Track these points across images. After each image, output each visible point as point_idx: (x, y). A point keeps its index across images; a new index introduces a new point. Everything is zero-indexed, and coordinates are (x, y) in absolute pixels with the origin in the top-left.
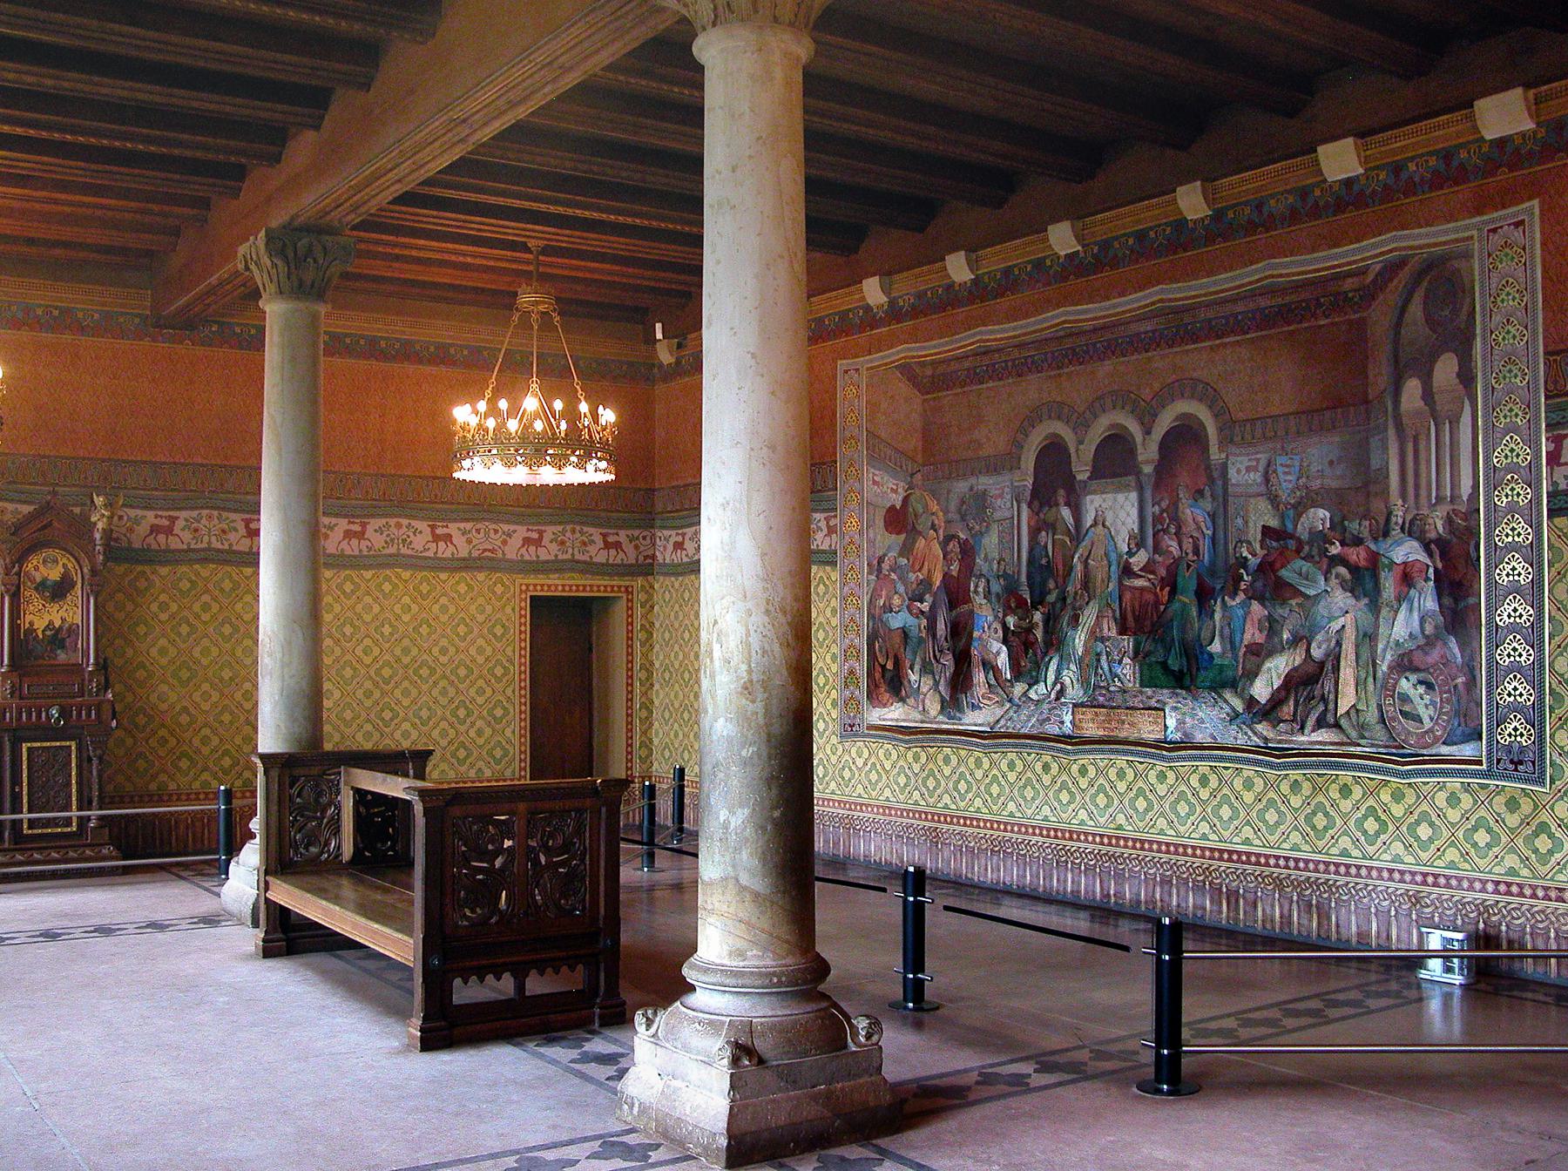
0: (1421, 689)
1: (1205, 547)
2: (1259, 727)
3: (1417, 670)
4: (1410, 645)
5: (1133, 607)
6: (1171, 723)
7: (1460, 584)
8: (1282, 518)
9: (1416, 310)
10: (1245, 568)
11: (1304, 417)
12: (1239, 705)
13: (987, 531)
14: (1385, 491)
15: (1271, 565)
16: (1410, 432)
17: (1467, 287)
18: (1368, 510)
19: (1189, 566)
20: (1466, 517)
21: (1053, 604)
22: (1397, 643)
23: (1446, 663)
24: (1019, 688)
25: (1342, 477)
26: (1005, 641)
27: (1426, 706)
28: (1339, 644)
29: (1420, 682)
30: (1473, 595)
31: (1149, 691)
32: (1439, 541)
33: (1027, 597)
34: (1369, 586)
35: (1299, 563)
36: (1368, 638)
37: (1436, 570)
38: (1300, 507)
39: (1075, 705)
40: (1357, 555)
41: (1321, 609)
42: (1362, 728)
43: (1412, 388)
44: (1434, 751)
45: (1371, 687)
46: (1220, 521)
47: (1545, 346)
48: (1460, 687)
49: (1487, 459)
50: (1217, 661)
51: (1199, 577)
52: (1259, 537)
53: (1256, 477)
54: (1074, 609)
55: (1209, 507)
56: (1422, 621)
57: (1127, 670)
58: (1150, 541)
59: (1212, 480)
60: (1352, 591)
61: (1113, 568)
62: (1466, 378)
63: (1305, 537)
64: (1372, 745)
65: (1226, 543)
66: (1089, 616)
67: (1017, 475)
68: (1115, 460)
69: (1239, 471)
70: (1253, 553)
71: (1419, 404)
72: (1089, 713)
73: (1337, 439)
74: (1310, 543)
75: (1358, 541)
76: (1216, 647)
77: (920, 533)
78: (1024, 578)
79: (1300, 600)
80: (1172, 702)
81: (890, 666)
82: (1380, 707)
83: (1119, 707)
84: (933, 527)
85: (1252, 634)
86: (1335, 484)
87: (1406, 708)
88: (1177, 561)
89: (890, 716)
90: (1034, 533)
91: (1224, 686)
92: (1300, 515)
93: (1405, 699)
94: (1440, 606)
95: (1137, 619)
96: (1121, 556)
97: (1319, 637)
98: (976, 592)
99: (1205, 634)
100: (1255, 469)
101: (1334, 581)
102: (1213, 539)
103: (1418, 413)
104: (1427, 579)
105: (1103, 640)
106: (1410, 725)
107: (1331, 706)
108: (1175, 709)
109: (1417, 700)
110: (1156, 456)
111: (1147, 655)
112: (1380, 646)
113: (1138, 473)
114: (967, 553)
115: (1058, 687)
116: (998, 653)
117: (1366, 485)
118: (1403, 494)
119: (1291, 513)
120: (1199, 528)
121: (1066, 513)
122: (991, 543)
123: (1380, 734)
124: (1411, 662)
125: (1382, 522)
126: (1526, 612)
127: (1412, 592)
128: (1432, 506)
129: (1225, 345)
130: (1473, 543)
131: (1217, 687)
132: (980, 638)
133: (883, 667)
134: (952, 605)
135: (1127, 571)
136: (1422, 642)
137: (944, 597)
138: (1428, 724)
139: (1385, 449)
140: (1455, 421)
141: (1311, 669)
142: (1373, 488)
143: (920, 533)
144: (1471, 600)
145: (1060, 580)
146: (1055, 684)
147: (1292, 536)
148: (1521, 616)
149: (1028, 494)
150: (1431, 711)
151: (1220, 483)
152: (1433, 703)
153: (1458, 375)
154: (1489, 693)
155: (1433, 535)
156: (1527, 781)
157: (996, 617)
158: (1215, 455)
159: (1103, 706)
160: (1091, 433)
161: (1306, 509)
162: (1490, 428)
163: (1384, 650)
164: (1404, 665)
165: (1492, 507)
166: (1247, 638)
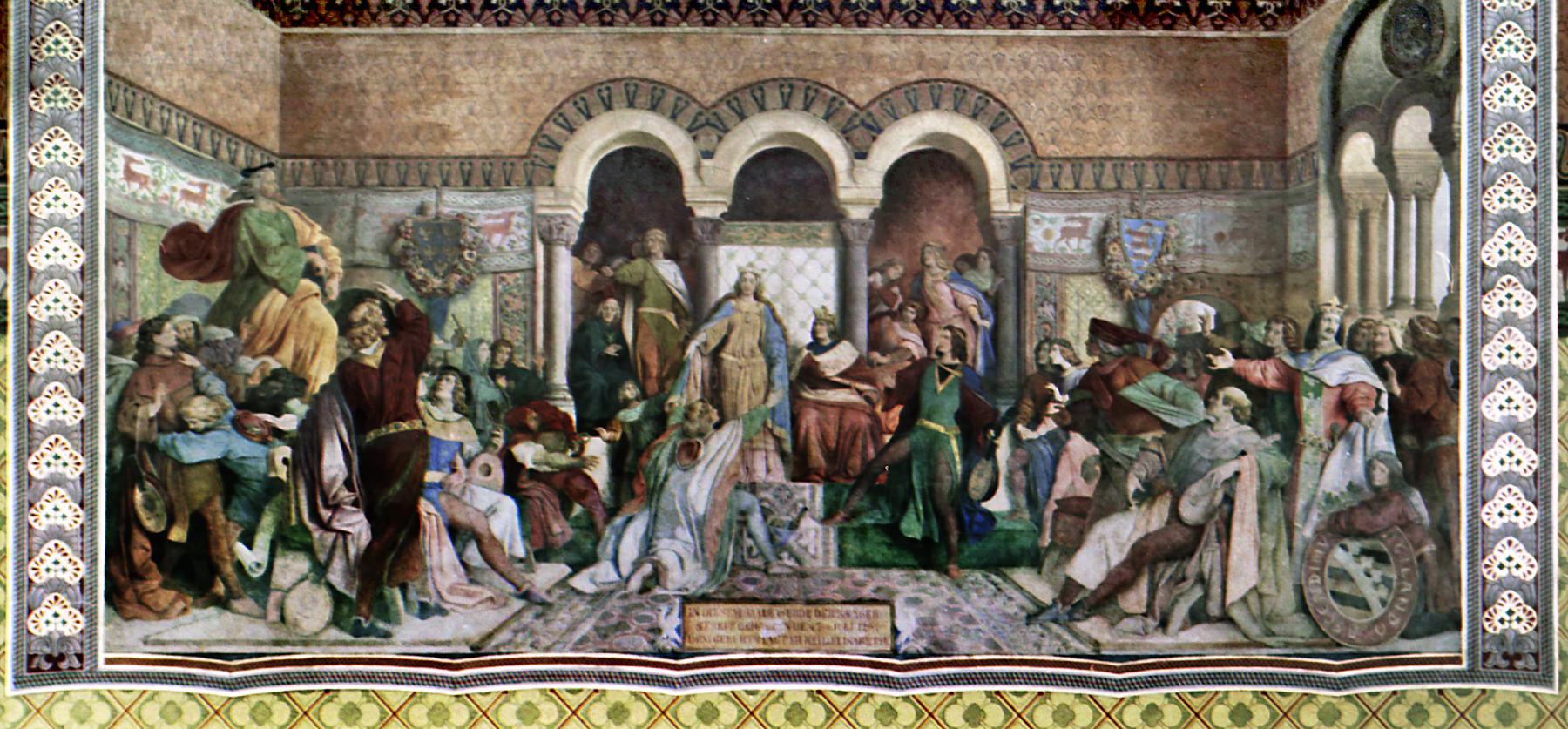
0: (1367, 562)
1: (976, 348)
2: (1084, 626)
3: (1361, 535)
4: (1348, 501)
5: (824, 440)
6: (907, 622)
7: (1427, 418)
8: (1131, 309)
9: (1369, 38)
10: (1059, 382)
11: (1172, 166)
12: (1044, 592)
13: (465, 286)
14: (1313, 285)
15: (1108, 379)
16: (1355, 208)
17: (1450, 21)
18: (1283, 309)
19: (944, 375)
20: (1439, 327)
21: (635, 426)
22: (1329, 499)
23: (1407, 524)
24: (547, 575)
25: (1240, 259)
26: (510, 488)
27: (1376, 585)
28: (1229, 500)
29: (1365, 552)
30: (1447, 433)
31: (860, 574)
32: (1397, 358)
33: (569, 408)
34: (1282, 417)
35: (1156, 380)
36: (1281, 489)
37: (1391, 396)
38: (1162, 298)
39: (686, 600)
40: (1264, 373)
41: (1199, 447)
42: (1267, 620)
43: (1359, 151)
44: (1387, 648)
45: (1284, 561)
46: (1009, 308)
47: (1560, 117)
48: (1430, 559)
49: (1474, 254)
50: (1001, 524)
51: (964, 390)
52: (1085, 336)
53: (1083, 246)
54: (685, 433)
55: (987, 284)
56: (1369, 467)
57: (815, 539)
58: (862, 330)
59: (993, 246)
60: (1253, 423)
61: (781, 369)
62: (1444, 141)
63: (1171, 340)
64: (1287, 645)
65: (1020, 343)
66: (722, 446)
67: (544, 197)
68: (785, 191)
69: (1047, 234)
70: (1076, 361)
71: (1372, 169)
72: (720, 614)
73: (1231, 204)
74: (1181, 350)
75: (1265, 353)
76: (999, 504)
77: (273, 283)
78: (560, 377)
79: (1159, 434)
80: (908, 591)
81: (178, 534)
82: (1299, 590)
83: (790, 601)
84: (311, 272)
85: (1070, 482)
86: (1225, 268)
87: (1345, 589)
88: (920, 366)
90: (589, 302)
91: (1014, 562)
92: (1163, 309)
93: (1342, 575)
94: (1398, 445)
95: (832, 455)
96: (797, 351)
97: (1194, 489)
98: (433, 398)
99: (978, 483)
100: (1081, 233)
101: (1220, 409)
102: (995, 334)
103: (1368, 182)
104: (1378, 410)
105: (753, 488)
106: (1351, 613)
107: (1216, 590)
108: (915, 602)
109: (1359, 576)
110: (878, 195)
111: (854, 514)
112: (1301, 502)
113: (836, 216)
114: (409, 330)
115: (647, 569)
116: (493, 510)
117: (1279, 275)
118: (1341, 290)
119: (1146, 304)
120: (964, 313)
121: (670, 272)
122: (474, 311)
123: (1299, 628)
124: (1349, 523)
125: (1305, 323)
126: (1528, 458)
127: (1355, 428)
128: (1388, 311)
129: (1029, 39)
130: (1448, 363)
131: (1001, 561)
132: (440, 485)
134: (360, 424)
135: (810, 376)
136: (1368, 494)
138: (1378, 611)
139: (1312, 221)
140: (1425, 198)
141: (1179, 536)
142: (1290, 279)
144: (1445, 441)
145: (652, 386)
146: (637, 565)
147: (1146, 339)
148: (1519, 462)
149: (573, 232)
150: (1383, 592)
151: (1011, 248)
152: (1386, 581)
153: (1432, 137)
154: (1472, 564)
155: (1387, 349)
156: (1528, 681)
157: (486, 445)
158: (1001, 201)
159: (754, 601)
160: (731, 141)
161: (1172, 300)
162: (1480, 213)
163: (1308, 509)
164: (1340, 526)
165: (1478, 317)
166: (1062, 488)
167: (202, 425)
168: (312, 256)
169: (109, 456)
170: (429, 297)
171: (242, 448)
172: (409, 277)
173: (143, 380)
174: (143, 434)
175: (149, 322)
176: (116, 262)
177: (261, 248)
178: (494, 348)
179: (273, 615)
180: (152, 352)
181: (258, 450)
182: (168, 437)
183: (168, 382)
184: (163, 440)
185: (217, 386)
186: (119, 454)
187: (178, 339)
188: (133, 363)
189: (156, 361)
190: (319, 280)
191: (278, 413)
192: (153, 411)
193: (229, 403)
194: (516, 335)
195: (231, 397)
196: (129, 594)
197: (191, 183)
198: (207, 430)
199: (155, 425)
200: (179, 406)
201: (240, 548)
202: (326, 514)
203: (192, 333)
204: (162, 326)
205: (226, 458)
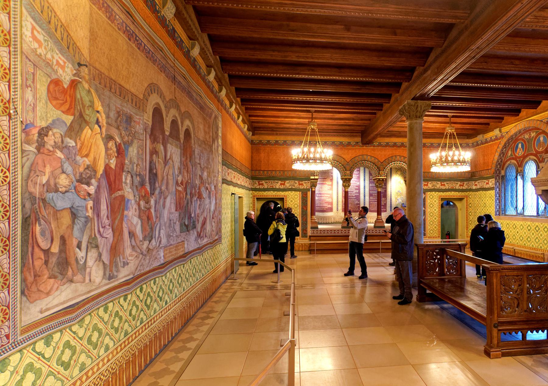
77: (87, 123)
81: (55, 249)
84: (98, 122)
89: (55, 302)
98: (126, 183)
133: (47, 252)
137: (104, 183)
143: (87, 123)
157: (136, 201)
167: (64, 189)
168: (98, 115)
169: (23, 206)
170: (125, 143)
171: (78, 202)
172: (121, 134)
173: (40, 162)
174: (40, 193)
175: (43, 129)
176: (27, 87)
177: (84, 106)
178: (137, 166)
179: (87, 280)
180: (44, 146)
181: (83, 203)
182: (51, 194)
183: (51, 165)
184: (49, 196)
185: (68, 168)
186: (28, 205)
187: (55, 142)
188: (35, 151)
189: (46, 151)
190: (100, 126)
191: (88, 184)
192: (44, 180)
193: (74, 179)
194: (140, 163)
195: (75, 175)
196: (34, 288)
197: (60, 58)
198: (66, 192)
199: (45, 187)
200: (55, 179)
201: (77, 249)
202: (101, 230)
203: (60, 140)
204: (48, 132)
205: (72, 207)
